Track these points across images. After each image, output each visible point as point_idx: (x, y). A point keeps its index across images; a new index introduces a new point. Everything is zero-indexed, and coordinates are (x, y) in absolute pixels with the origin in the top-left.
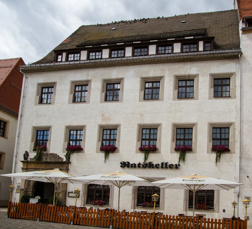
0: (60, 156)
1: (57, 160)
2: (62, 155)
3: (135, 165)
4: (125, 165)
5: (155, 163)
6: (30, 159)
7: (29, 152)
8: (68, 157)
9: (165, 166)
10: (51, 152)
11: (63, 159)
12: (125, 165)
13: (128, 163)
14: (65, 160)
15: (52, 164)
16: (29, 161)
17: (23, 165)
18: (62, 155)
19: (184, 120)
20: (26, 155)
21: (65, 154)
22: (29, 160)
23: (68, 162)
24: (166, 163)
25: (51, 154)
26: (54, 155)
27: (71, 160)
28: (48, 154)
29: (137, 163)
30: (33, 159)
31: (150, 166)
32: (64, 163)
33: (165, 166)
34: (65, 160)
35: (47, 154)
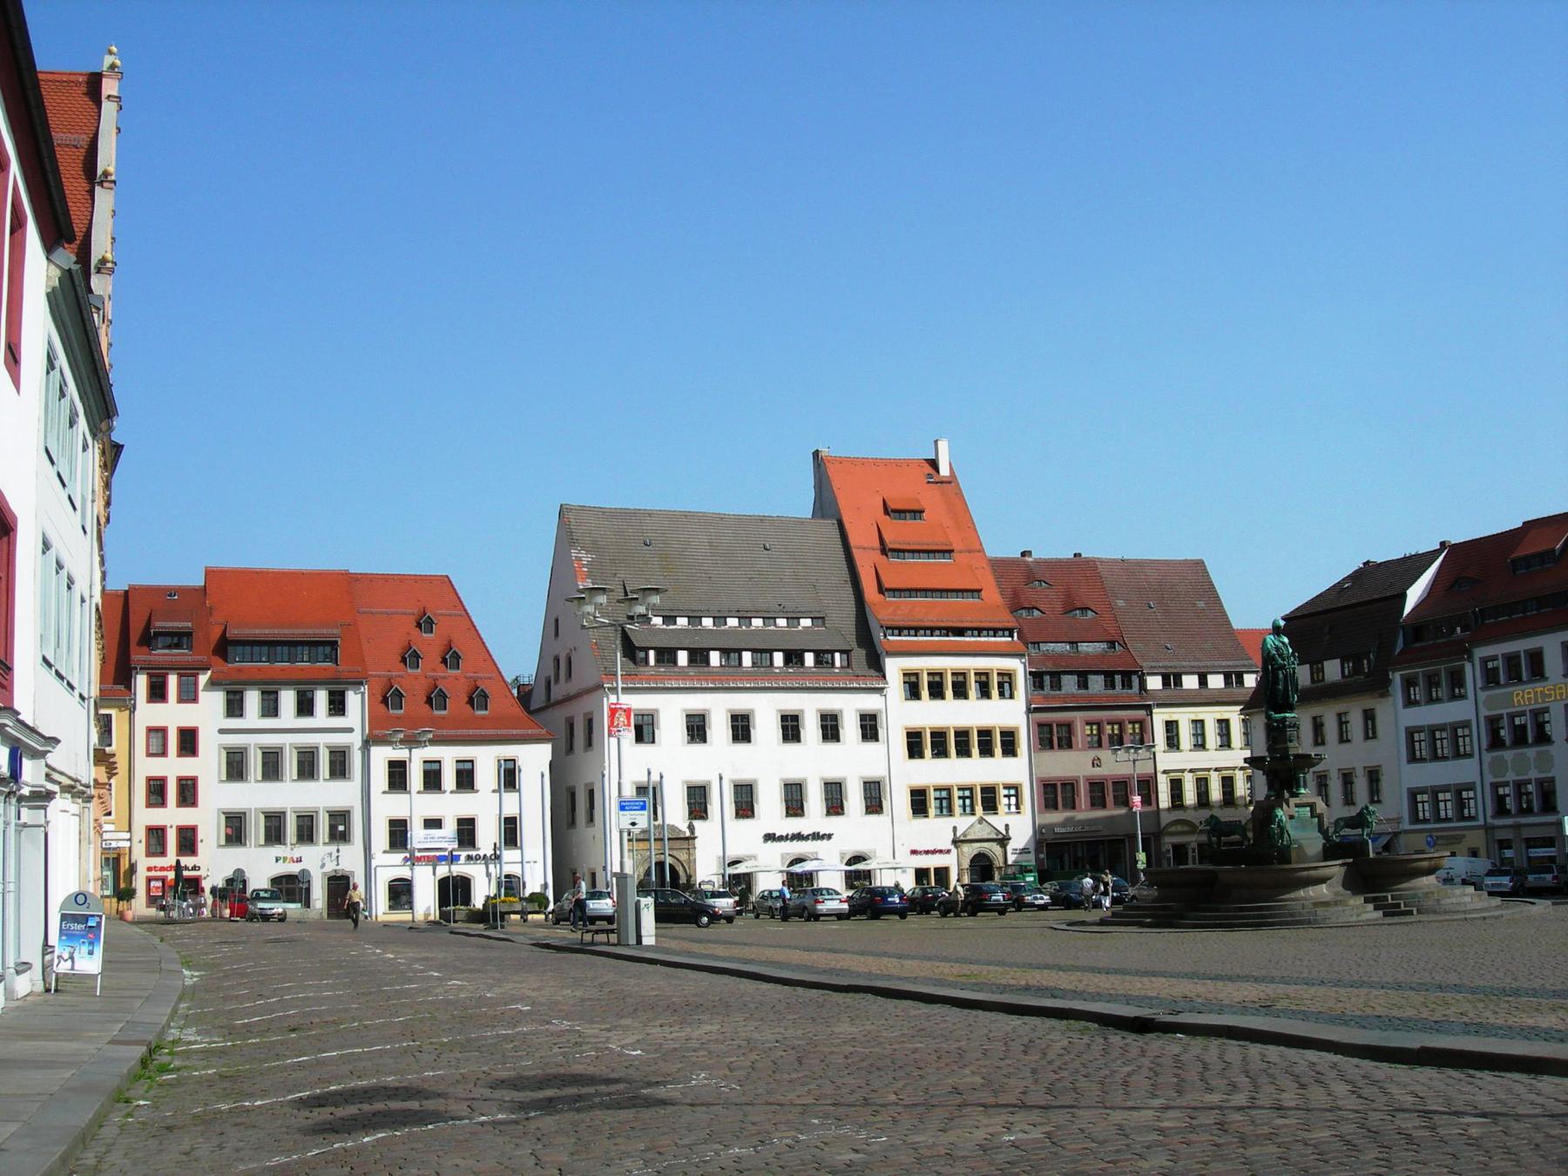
2: (683, 826)
3: (782, 836)
4: (770, 837)
5: (805, 833)
8: (691, 828)
9: (816, 836)
12: (770, 837)
13: (774, 834)
14: (688, 834)
18: (683, 826)
19: (833, 774)
21: (687, 824)
24: (818, 833)
26: (673, 828)
29: (784, 835)
31: (798, 837)
33: (816, 836)
34: (688, 834)
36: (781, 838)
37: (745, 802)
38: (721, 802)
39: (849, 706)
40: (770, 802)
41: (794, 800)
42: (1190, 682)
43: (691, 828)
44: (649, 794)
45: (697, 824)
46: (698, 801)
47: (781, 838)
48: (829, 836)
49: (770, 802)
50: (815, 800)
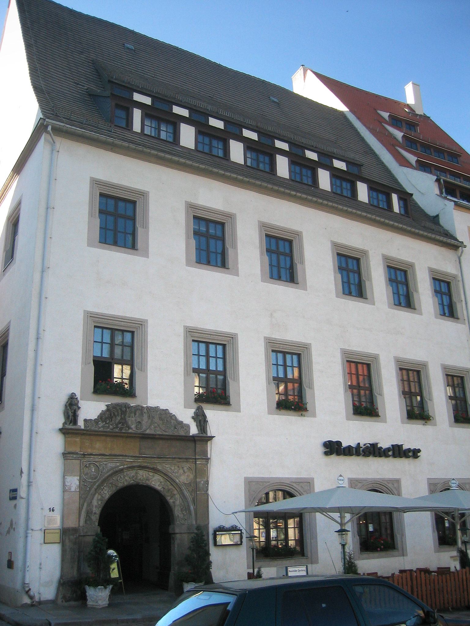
0: (180, 418)
1: (170, 432)
6: (85, 420)
7: (79, 399)
10: (152, 402)
11: (188, 426)
14: (194, 430)
15: (161, 442)
16: (83, 427)
17: (66, 443)
21: (191, 412)
22: (81, 424)
25: (149, 409)
27: (212, 430)
28: (142, 407)
29: (354, 445)
30: (96, 421)
32: (194, 439)
34: (194, 430)
35: (140, 410)
36: (349, 451)
47: (349, 451)
48: (415, 453)
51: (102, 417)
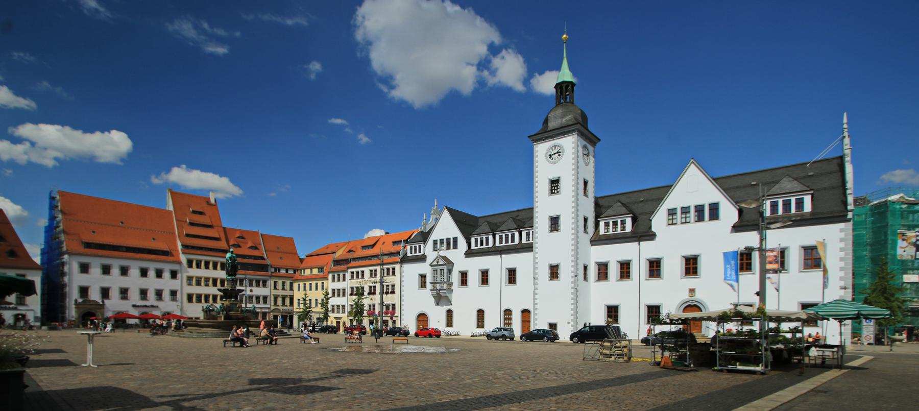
8: (103, 301)
14: (101, 303)
18: (100, 301)
20: (76, 301)
23: (103, 305)
34: (101, 303)
37: (124, 293)
38: (115, 294)
39: (167, 268)
40: (135, 297)
41: (144, 293)
42: (283, 271)
43: (103, 301)
44: (84, 291)
45: (106, 301)
46: (105, 293)
49: (135, 297)
50: (151, 295)
51: (82, 302)
